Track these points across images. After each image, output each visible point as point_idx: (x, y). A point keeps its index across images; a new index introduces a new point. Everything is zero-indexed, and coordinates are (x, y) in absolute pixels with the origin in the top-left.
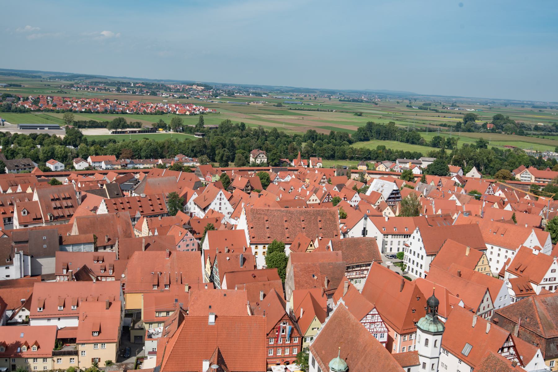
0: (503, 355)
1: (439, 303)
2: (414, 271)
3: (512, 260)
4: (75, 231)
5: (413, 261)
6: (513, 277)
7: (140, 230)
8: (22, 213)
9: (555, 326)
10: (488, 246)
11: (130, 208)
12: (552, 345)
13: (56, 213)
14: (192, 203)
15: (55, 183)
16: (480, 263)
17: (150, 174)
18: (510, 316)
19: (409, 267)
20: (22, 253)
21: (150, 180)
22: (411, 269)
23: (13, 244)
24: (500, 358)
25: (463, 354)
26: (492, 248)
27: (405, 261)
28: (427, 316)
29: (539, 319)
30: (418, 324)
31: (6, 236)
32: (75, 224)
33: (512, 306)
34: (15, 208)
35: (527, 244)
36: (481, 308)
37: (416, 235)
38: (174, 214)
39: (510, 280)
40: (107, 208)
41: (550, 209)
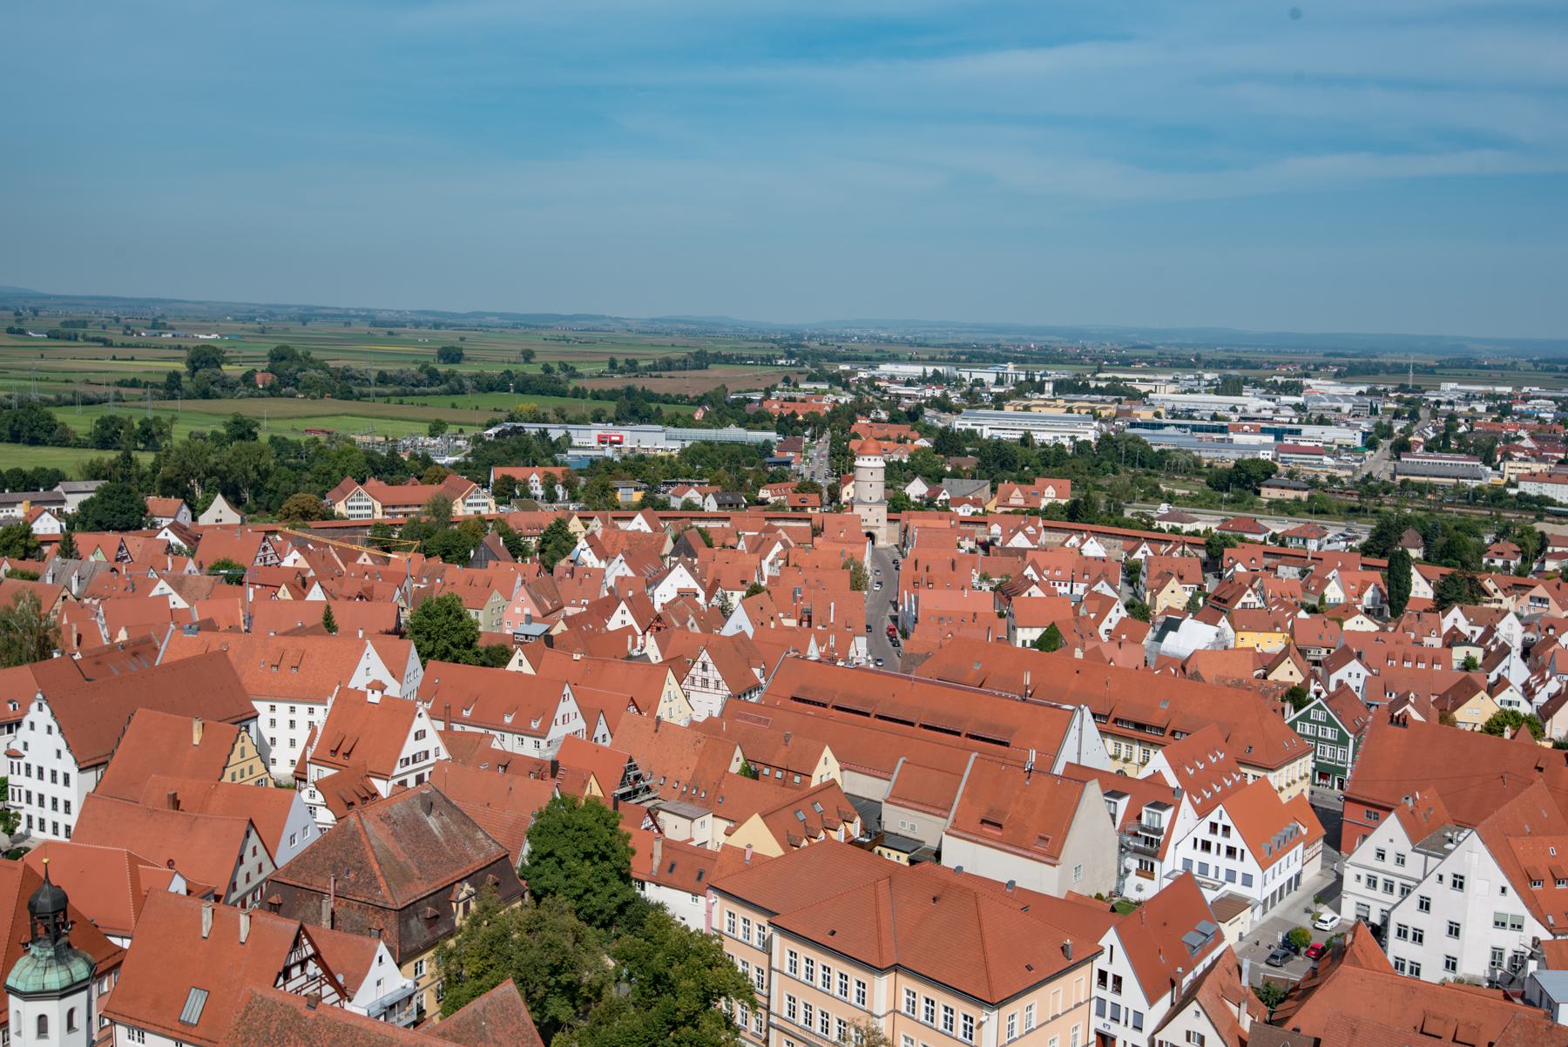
0: (290, 986)
1: (66, 899)
2: (49, 826)
3: (320, 731)
5: (41, 798)
6: (328, 772)
9: (416, 871)
10: (261, 707)
12: (413, 922)
16: (235, 757)
18: (308, 880)
19: (30, 818)
22: (36, 823)
24: (279, 998)
25: (184, 1023)
26: (273, 708)
27: (16, 803)
28: (34, 949)
29: (376, 867)
30: (10, 982)
33: (313, 849)
35: (358, 681)
36: (241, 879)
37: (40, 716)
39: (318, 785)
41: (419, 581)
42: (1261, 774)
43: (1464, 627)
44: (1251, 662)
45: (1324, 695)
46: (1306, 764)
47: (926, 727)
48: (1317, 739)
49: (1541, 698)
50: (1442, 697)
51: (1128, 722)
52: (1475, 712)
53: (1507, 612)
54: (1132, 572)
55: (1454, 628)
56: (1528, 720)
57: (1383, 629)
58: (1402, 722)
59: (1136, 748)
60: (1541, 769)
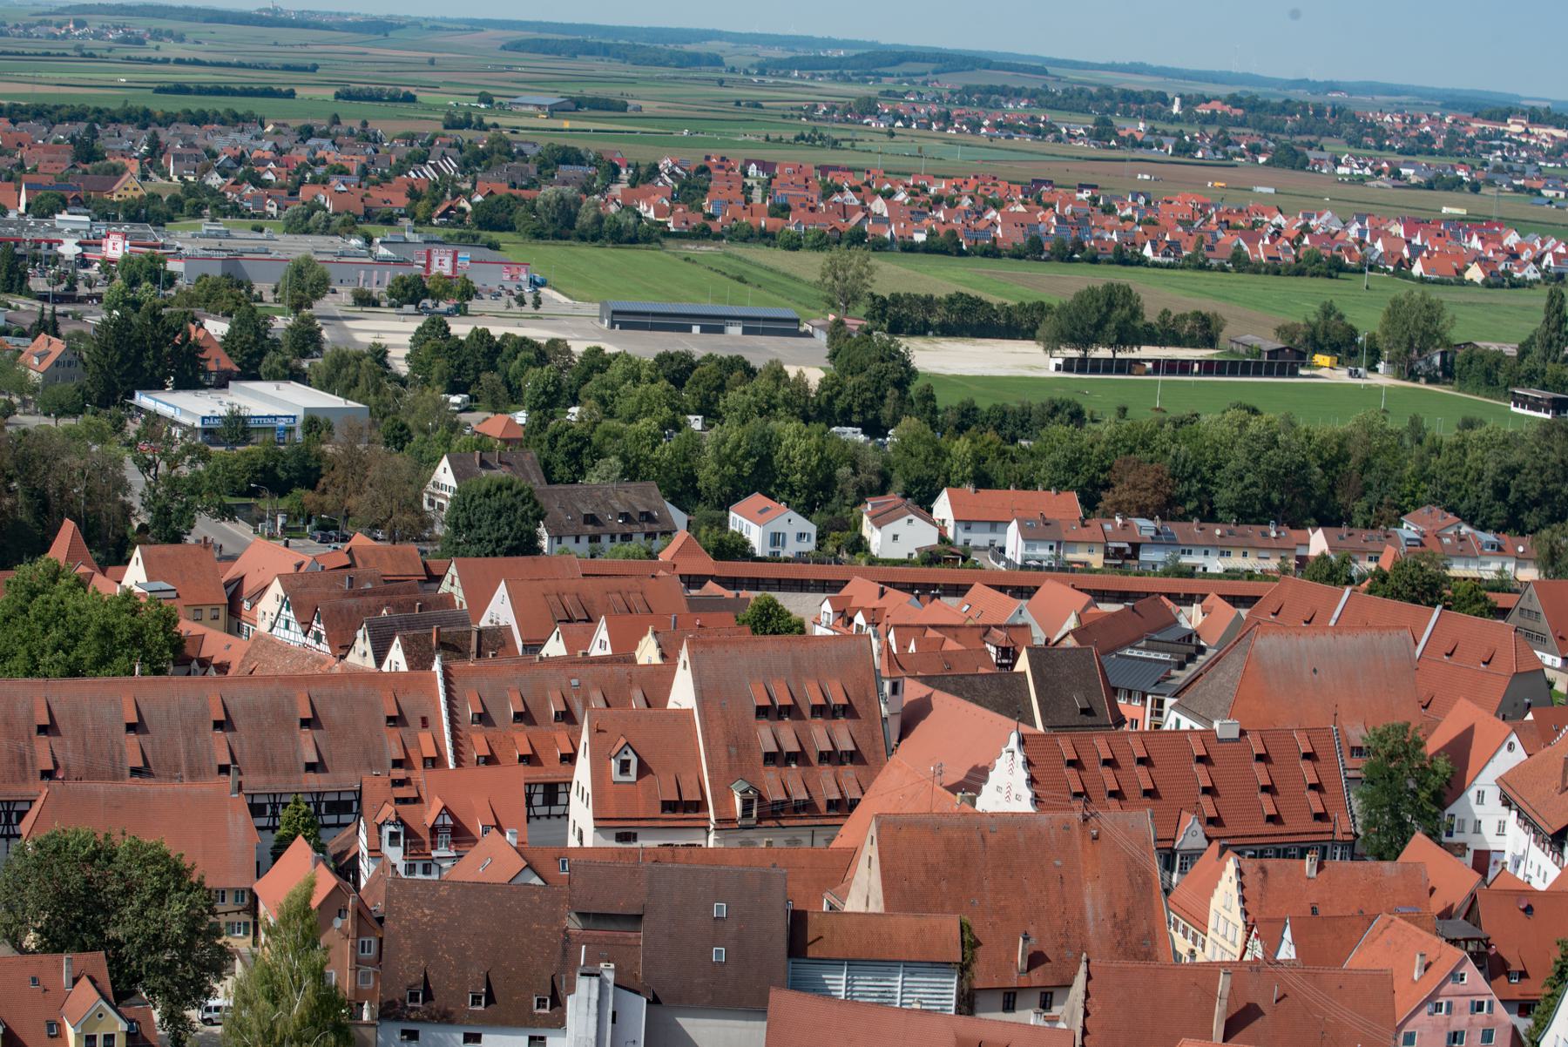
4: (864, 892)
7: (1199, 923)
8: (614, 765)
11: (1147, 793)
13: (774, 783)
14: (1492, 795)
15: (770, 622)
17: (1263, 611)
20: (610, 976)
21: (1270, 644)
23: (574, 924)
31: (536, 881)
32: (870, 851)
34: (585, 737)
38: (1389, 851)
40: (1032, 781)
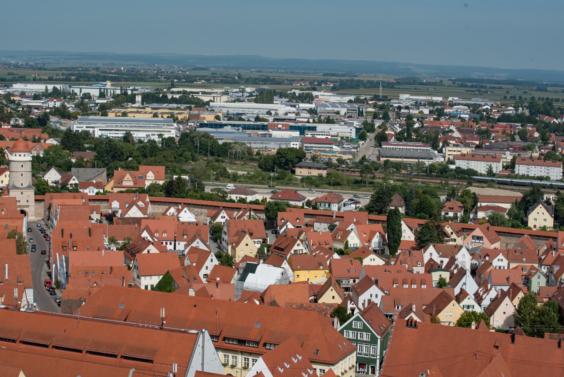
42: (327, 368)
43: (437, 258)
44: (307, 292)
45: (357, 311)
46: (352, 359)
47: (91, 353)
48: (357, 341)
49: (486, 302)
50: (429, 306)
51: (233, 340)
52: (450, 314)
53: (461, 247)
54: (216, 233)
55: (431, 260)
56: (481, 316)
57: (388, 263)
58: (411, 324)
59: (240, 357)
60: (497, 347)
